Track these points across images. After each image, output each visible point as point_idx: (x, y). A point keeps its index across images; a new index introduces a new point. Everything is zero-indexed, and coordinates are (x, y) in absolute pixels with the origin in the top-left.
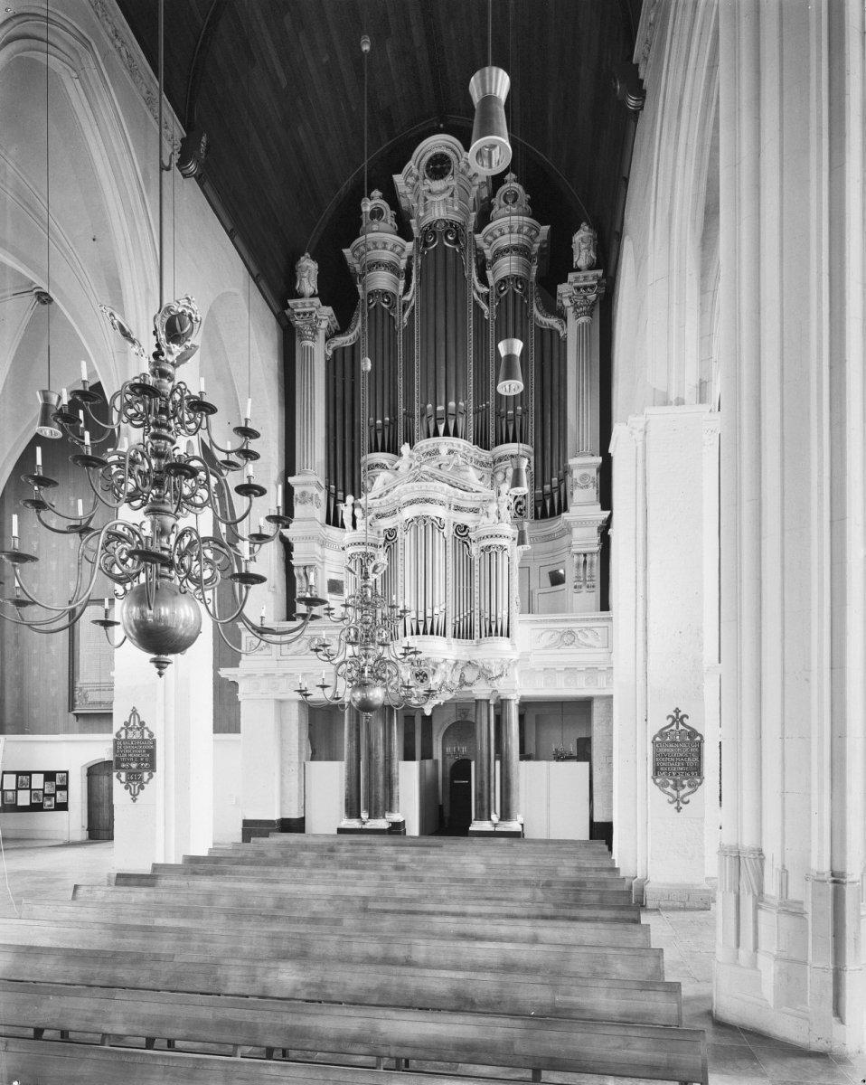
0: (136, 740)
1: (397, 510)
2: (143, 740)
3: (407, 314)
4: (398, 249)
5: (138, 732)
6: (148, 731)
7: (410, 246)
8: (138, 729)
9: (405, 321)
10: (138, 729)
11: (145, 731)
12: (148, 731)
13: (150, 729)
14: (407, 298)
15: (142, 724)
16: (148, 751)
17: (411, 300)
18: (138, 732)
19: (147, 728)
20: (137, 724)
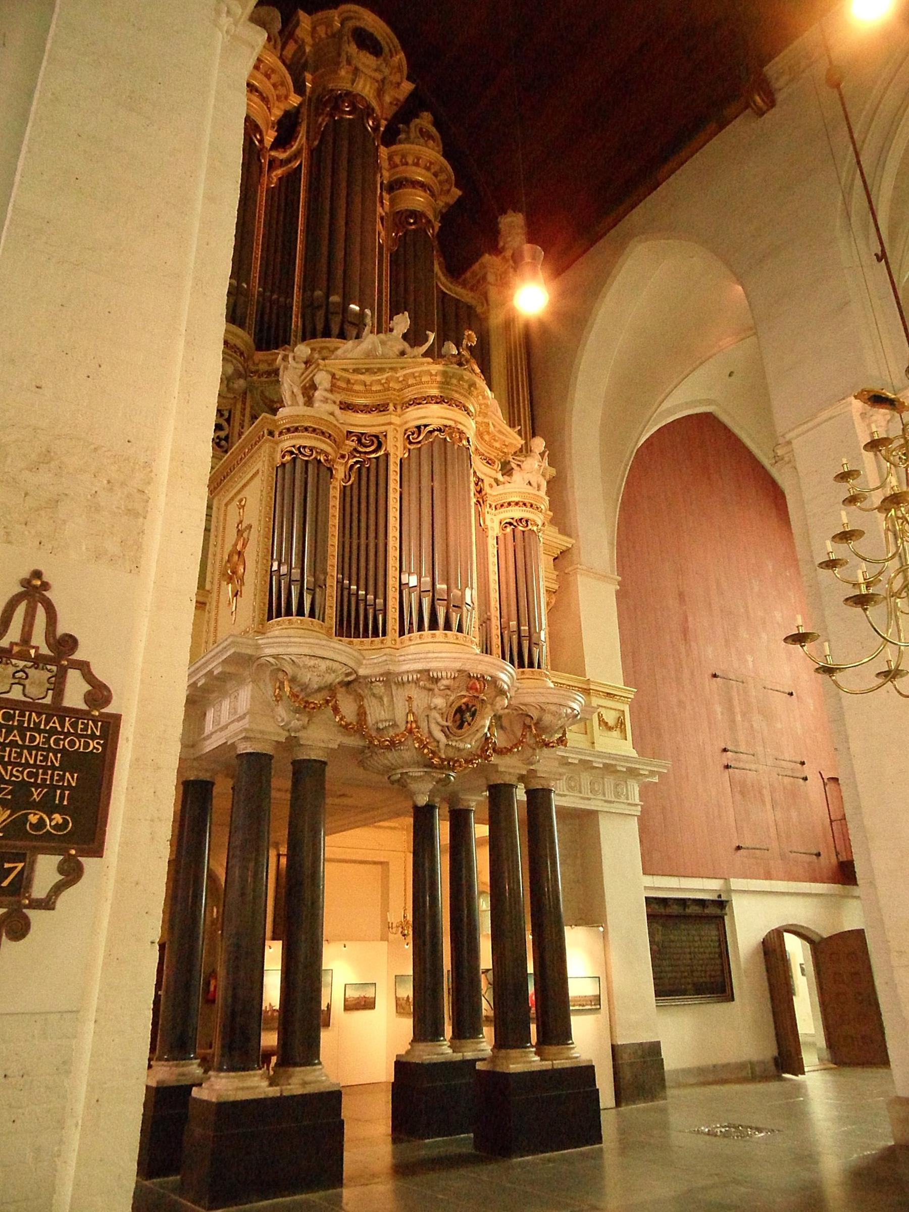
0: (23, 707)
1: (391, 407)
2: (59, 711)
3: (279, 172)
4: (282, 91)
5: (40, 676)
6: (88, 676)
7: (295, 100)
8: (39, 661)
9: (275, 180)
10: (39, 661)
11: (74, 676)
12: (88, 676)
13: (98, 672)
14: (282, 156)
15: (69, 643)
16: (72, 760)
17: (289, 160)
18: (40, 676)
19: (84, 667)
20: (39, 639)
